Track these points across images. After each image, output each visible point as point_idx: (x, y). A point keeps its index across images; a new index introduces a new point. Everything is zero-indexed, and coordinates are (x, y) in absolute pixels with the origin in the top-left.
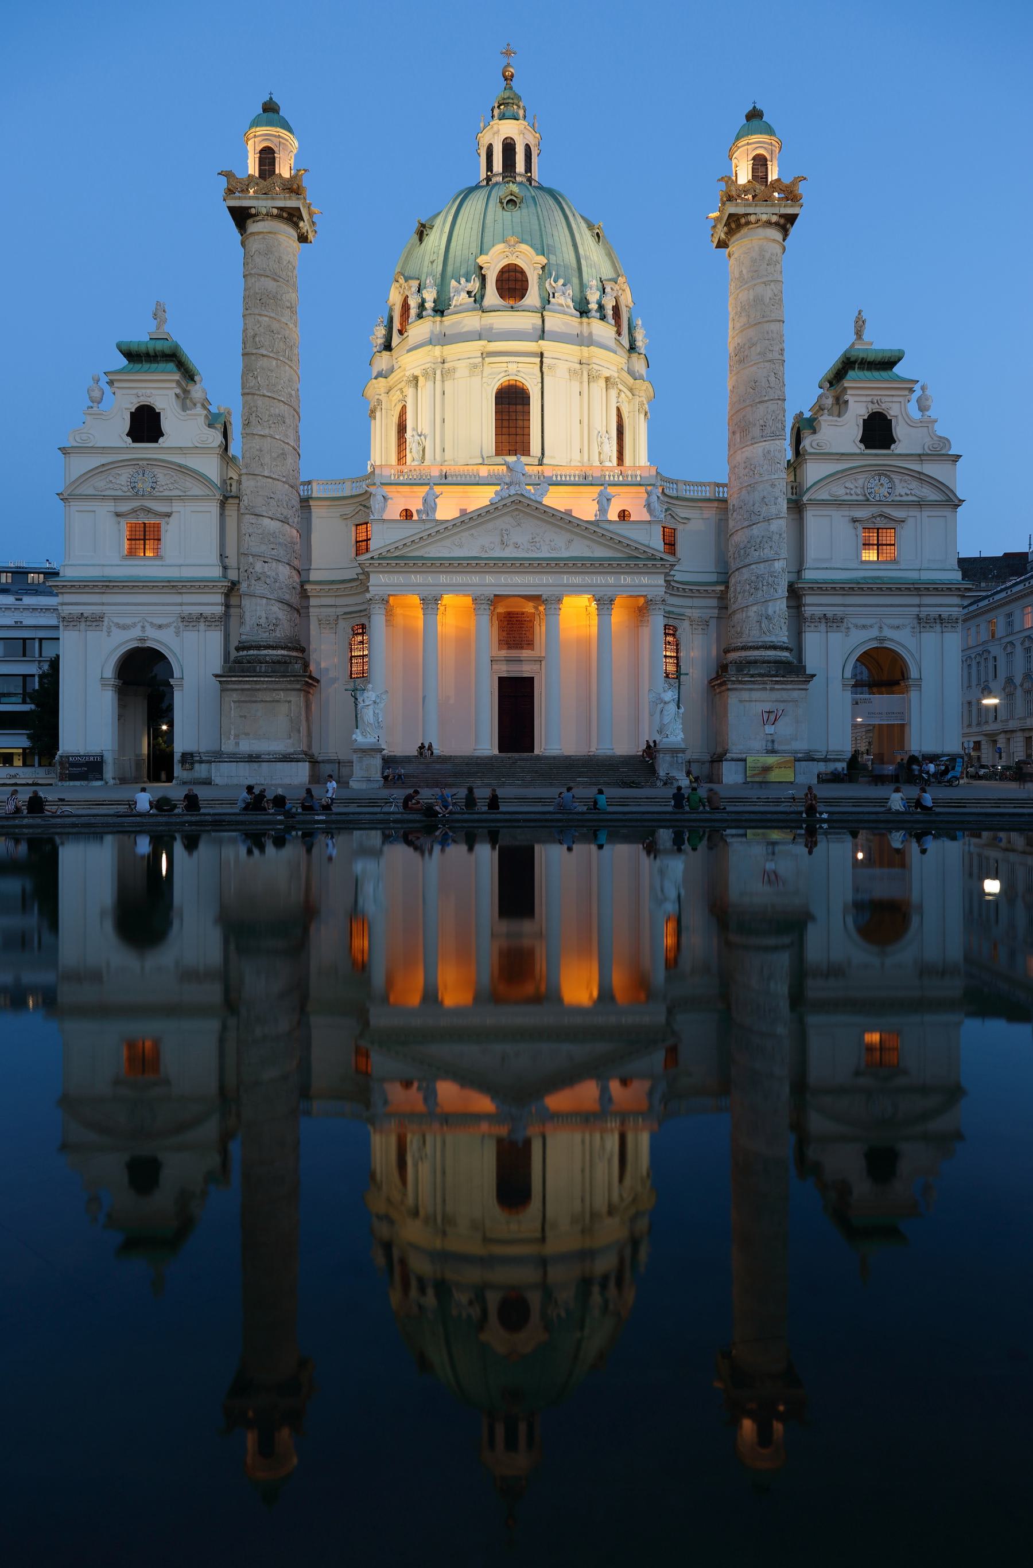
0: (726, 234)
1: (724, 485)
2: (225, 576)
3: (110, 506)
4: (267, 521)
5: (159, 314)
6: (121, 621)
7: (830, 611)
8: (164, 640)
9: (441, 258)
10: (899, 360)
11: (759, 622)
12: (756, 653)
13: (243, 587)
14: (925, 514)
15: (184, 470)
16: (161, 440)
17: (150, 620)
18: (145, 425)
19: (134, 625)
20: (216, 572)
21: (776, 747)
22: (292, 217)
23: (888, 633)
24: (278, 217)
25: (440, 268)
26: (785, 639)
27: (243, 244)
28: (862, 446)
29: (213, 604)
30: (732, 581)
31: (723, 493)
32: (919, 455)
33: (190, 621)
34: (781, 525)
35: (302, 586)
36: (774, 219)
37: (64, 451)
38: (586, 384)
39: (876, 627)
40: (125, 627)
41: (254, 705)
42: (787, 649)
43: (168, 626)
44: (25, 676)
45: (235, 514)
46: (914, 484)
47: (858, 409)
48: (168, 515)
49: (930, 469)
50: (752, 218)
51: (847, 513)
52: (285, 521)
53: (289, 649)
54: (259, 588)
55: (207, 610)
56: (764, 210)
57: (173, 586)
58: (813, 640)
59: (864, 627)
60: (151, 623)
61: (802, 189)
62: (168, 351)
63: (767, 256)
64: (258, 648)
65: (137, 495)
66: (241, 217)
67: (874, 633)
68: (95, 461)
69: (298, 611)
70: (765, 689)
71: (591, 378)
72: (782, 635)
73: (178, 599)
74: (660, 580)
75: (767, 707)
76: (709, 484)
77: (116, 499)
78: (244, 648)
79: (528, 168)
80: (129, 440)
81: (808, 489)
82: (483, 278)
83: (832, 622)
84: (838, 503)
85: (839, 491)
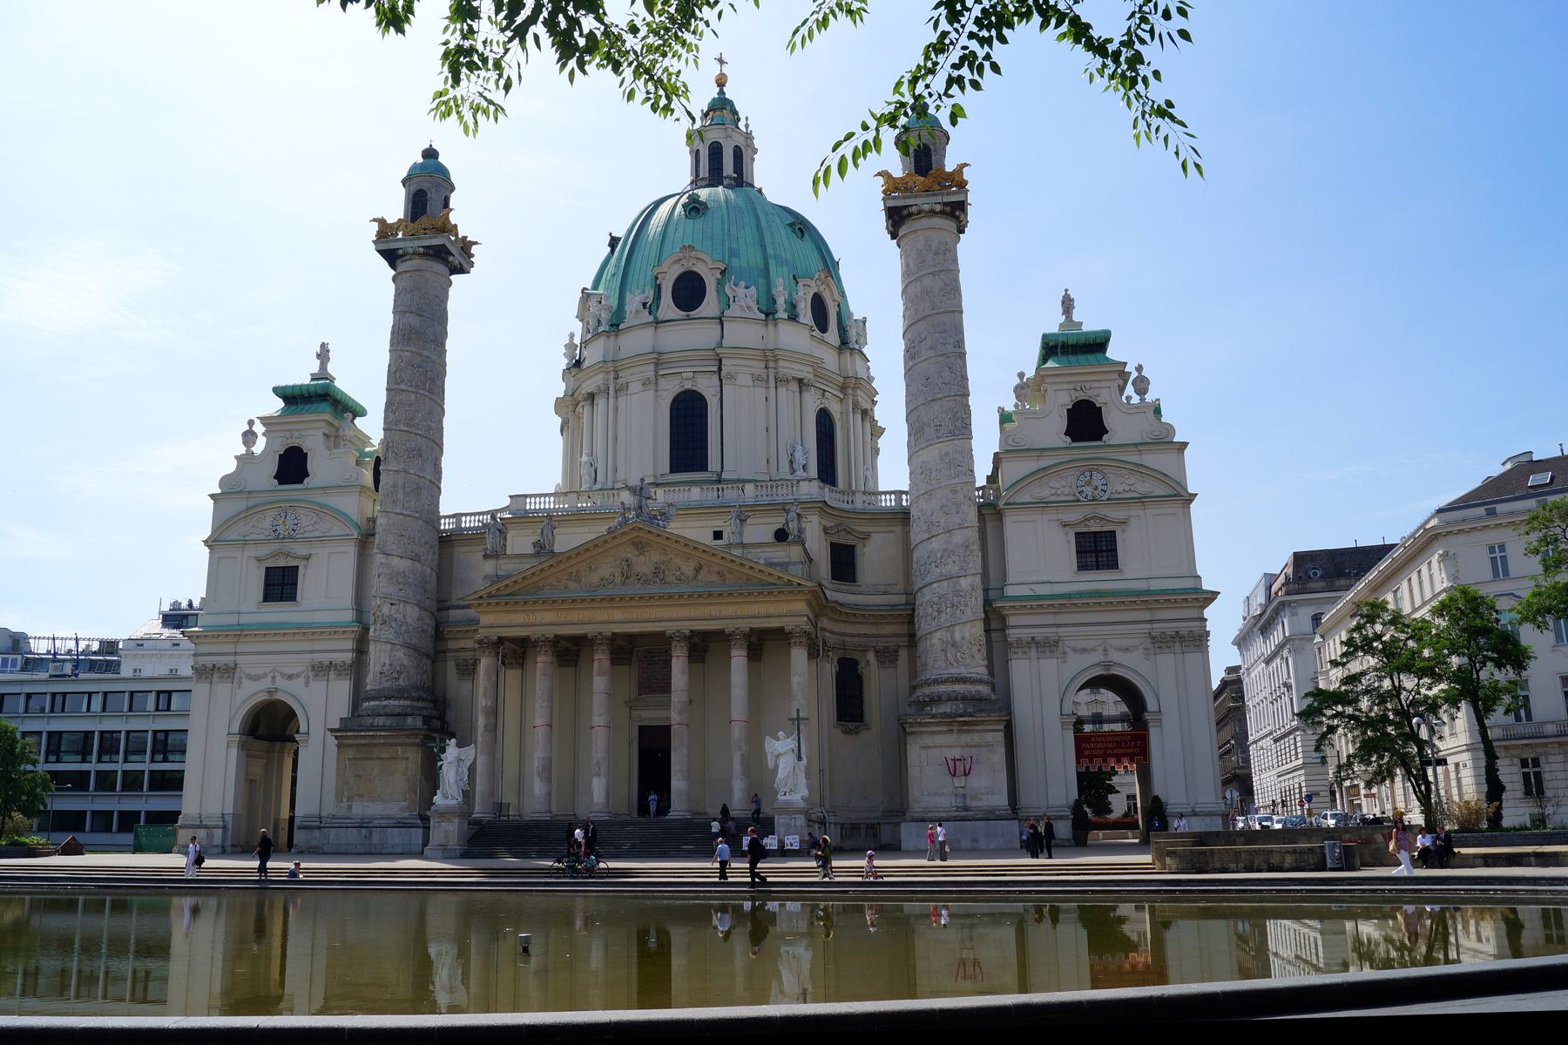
3: (252, 552)
4: (395, 561)
5: (324, 354)
7: (1040, 633)
10: (1108, 340)
12: (942, 688)
15: (324, 510)
18: (292, 466)
19: (265, 675)
20: (349, 616)
21: (969, 803)
22: (439, 254)
23: (1115, 656)
26: (981, 670)
27: (394, 279)
28: (1068, 439)
33: (321, 670)
35: (437, 629)
36: (938, 208)
37: (212, 496)
38: (772, 390)
39: (1100, 650)
40: (256, 678)
42: (980, 681)
43: (298, 675)
50: (914, 209)
51: (1054, 517)
52: (416, 558)
53: (413, 699)
54: (387, 633)
56: (924, 200)
58: (1021, 671)
59: (1084, 650)
60: (283, 675)
61: (967, 174)
62: (320, 392)
63: (935, 245)
66: (391, 256)
67: (1097, 657)
68: (238, 505)
69: (428, 656)
70: (951, 731)
74: (802, 607)
75: (957, 753)
77: (256, 542)
82: (658, 288)
83: (1048, 646)
84: (1043, 505)
85: (1042, 491)
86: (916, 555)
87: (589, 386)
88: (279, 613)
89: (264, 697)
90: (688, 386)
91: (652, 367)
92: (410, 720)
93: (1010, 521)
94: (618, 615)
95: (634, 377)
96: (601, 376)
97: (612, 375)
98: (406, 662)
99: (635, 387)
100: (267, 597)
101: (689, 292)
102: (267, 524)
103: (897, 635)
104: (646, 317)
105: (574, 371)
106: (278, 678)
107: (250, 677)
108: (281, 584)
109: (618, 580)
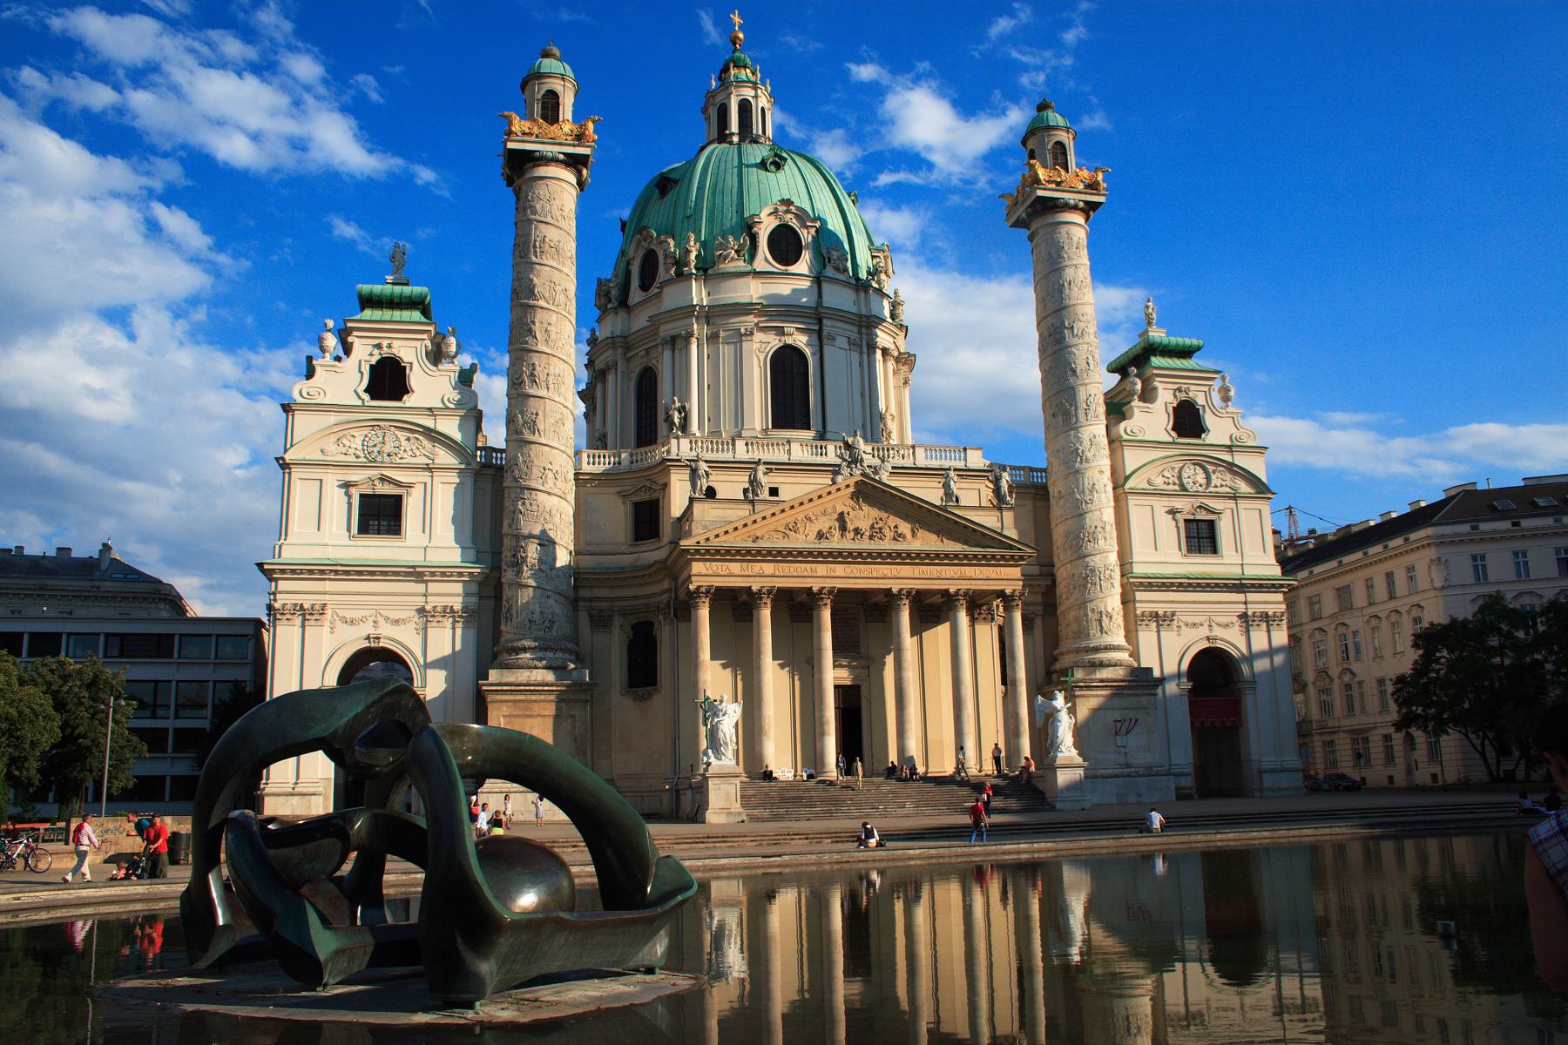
0: (1029, 215)
1: (1044, 470)
8: (404, 638)
11: (1100, 621)
14: (1242, 504)
16: (405, 398)
17: (385, 613)
18: (388, 380)
19: (363, 620)
23: (1217, 632)
24: (562, 162)
28: (1174, 434)
31: (1039, 478)
32: (1229, 447)
34: (1108, 515)
41: (529, 720)
44: (156, 682)
47: (1166, 395)
49: (1241, 460)
57: (416, 574)
65: (372, 463)
72: (1118, 638)
73: (421, 588)
76: (1023, 468)
80: (366, 397)
81: (1127, 478)
82: (754, 238)
87: (667, 330)
88: (378, 549)
89: (366, 644)
90: (789, 341)
93: (1133, 501)
94: (840, 570)
98: (558, 610)
102: (358, 443)
103: (1034, 604)
104: (741, 265)
105: (622, 315)
106: (381, 620)
109: (837, 534)
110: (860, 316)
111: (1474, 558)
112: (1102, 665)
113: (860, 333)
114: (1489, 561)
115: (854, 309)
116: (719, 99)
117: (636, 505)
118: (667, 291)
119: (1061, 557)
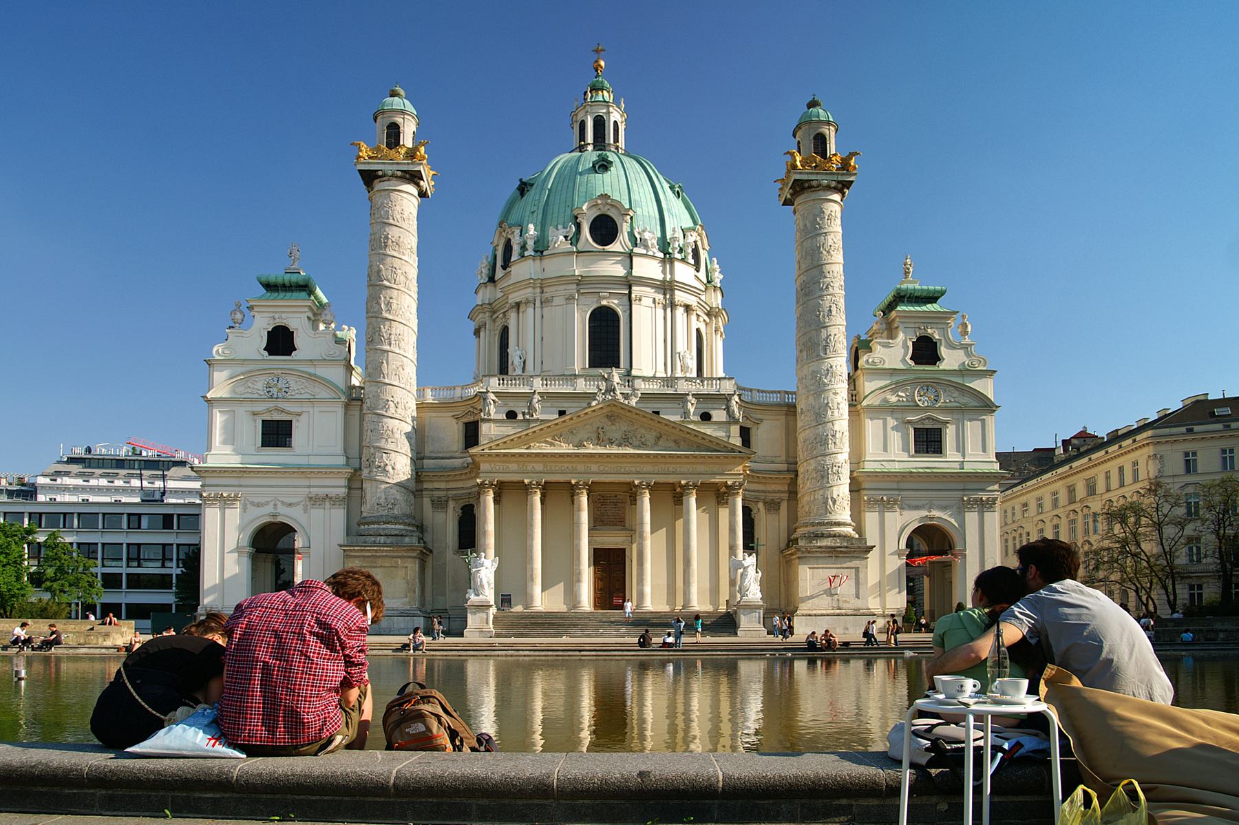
2: (347, 464)
6: (256, 500)
9: (541, 211)
11: (826, 503)
13: (365, 472)
20: (341, 460)
25: (540, 216)
29: (338, 486)
30: (801, 470)
31: (790, 399)
45: (357, 414)
46: (956, 394)
48: (299, 414)
53: (405, 524)
55: (333, 492)
64: (378, 523)
71: (673, 306)
73: (306, 482)
78: (364, 524)
79: (616, 140)
86: (801, 438)
88: (276, 456)
90: (604, 303)
91: (575, 286)
92: (407, 539)
95: (557, 293)
96: (530, 290)
97: (538, 290)
99: (558, 301)
100: (265, 443)
101: (605, 229)
104: (568, 246)
107: (253, 504)
108: (276, 434)
110: (664, 281)
111: (1187, 454)
112: (823, 536)
113: (665, 294)
114: (1199, 458)
115: (660, 277)
116: (580, 117)
117: (467, 425)
118: (514, 269)
119: (801, 456)
